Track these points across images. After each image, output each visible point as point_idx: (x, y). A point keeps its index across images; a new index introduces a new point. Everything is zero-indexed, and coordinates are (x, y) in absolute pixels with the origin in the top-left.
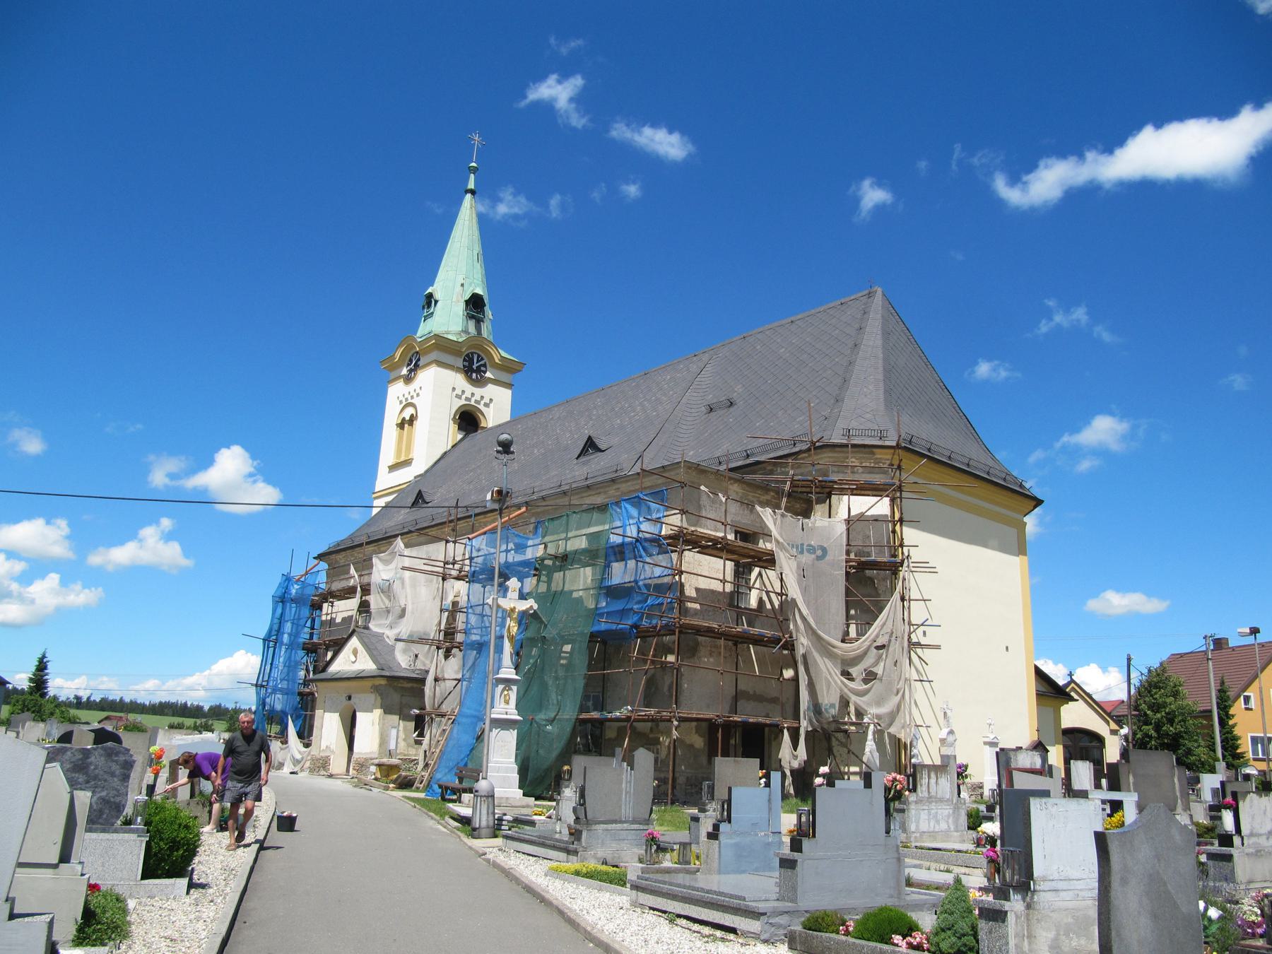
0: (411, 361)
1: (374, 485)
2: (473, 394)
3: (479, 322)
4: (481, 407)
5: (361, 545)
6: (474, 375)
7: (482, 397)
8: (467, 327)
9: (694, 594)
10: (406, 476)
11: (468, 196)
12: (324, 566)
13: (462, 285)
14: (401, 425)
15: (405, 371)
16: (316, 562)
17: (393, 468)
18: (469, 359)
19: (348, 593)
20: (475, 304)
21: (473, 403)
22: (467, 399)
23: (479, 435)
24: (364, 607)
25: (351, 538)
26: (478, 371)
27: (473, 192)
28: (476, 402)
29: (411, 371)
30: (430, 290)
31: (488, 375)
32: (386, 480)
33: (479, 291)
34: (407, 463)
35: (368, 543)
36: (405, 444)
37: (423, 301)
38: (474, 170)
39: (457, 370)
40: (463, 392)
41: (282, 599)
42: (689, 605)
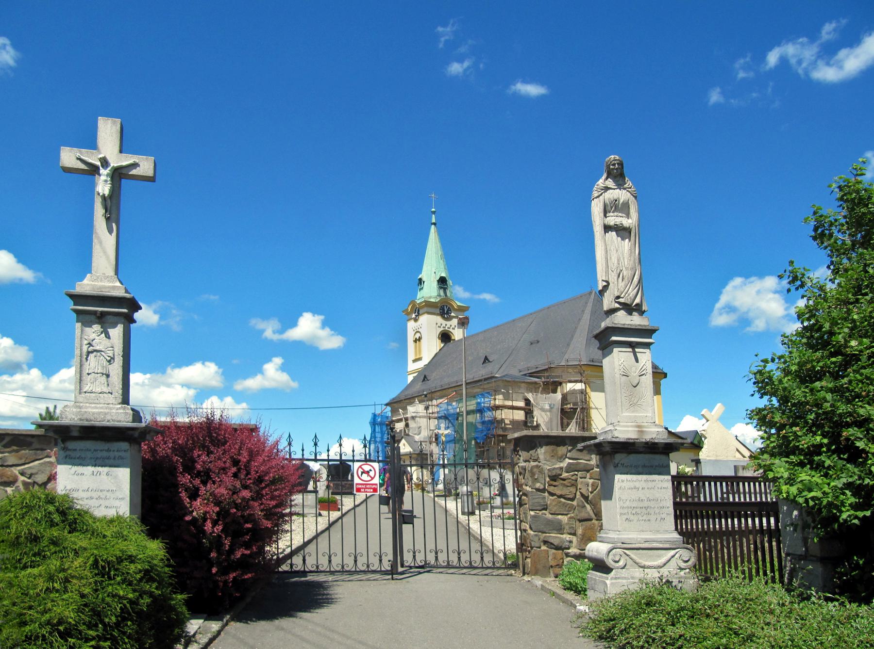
0: (416, 311)
1: (407, 368)
2: (446, 325)
3: (445, 289)
4: (451, 330)
5: (402, 400)
6: (446, 316)
7: (451, 326)
8: (439, 293)
9: (509, 423)
10: (420, 365)
11: (433, 226)
12: (389, 408)
13: (435, 273)
14: (415, 341)
15: (414, 316)
16: (385, 407)
17: (414, 361)
18: (442, 308)
19: (400, 420)
20: (442, 281)
21: (447, 329)
22: (443, 327)
23: (451, 344)
24: (407, 425)
25: (398, 396)
26: (448, 313)
27: (435, 224)
28: (448, 328)
29: (416, 316)
30: (420, 277)
31: (452, 314)
32: (412, 367)
33: (443, 275)
34: (420, 359)
35: (405, 400)
36: (418, 350)
37: (418, 281)
38: (434, 213)
39: (437, 315)
40: (441, 324)
41: (374, 423)
42: (507, 426)
